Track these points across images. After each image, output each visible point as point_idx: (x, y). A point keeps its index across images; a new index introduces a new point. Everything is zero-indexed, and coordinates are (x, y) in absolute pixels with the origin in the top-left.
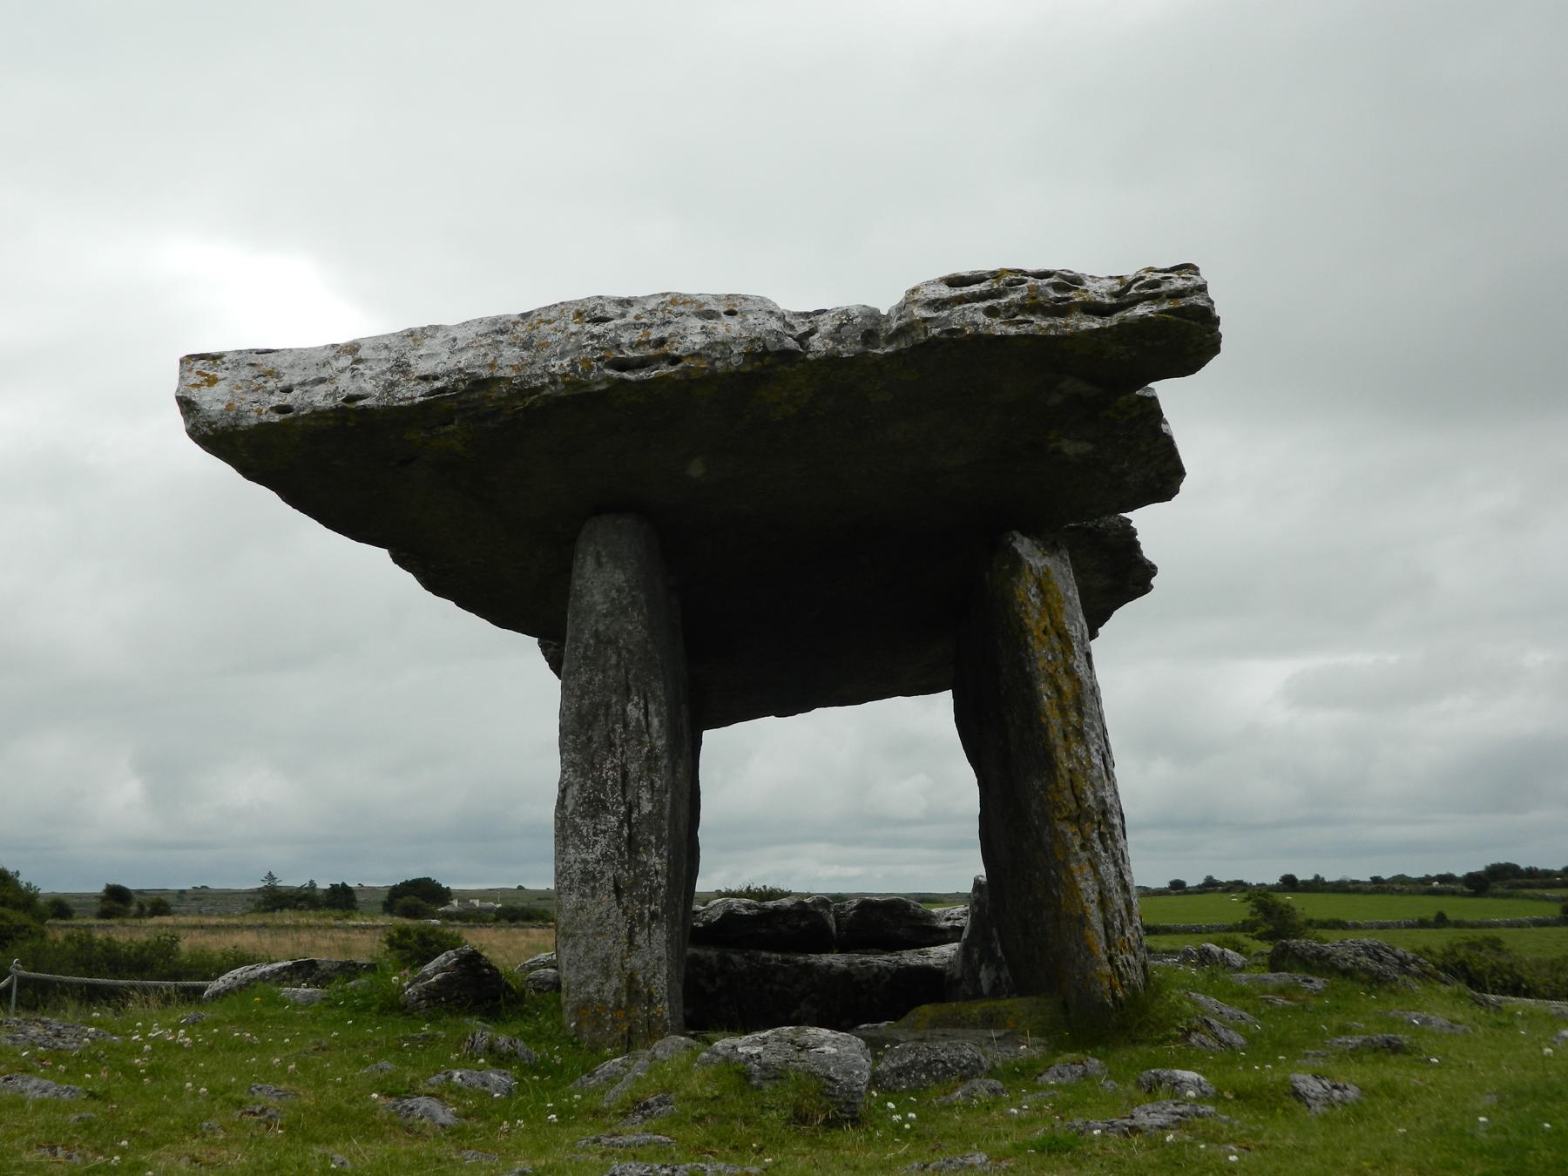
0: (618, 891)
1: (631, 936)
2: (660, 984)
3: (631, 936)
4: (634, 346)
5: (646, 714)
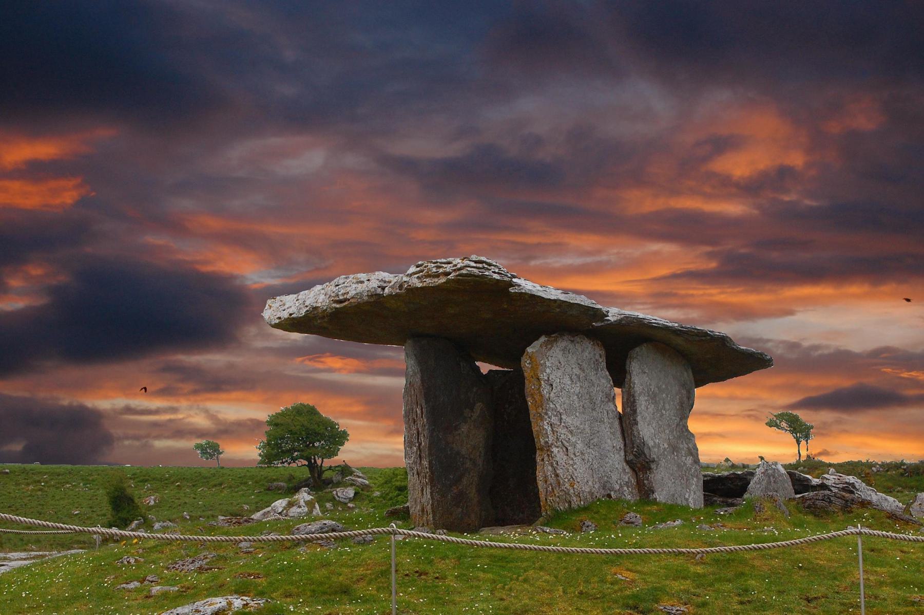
0: (418, 474)
1: (422, 490)
2: (429, 508)
3: (422, 490)
4: (343, 294)
5: (422, 413)
